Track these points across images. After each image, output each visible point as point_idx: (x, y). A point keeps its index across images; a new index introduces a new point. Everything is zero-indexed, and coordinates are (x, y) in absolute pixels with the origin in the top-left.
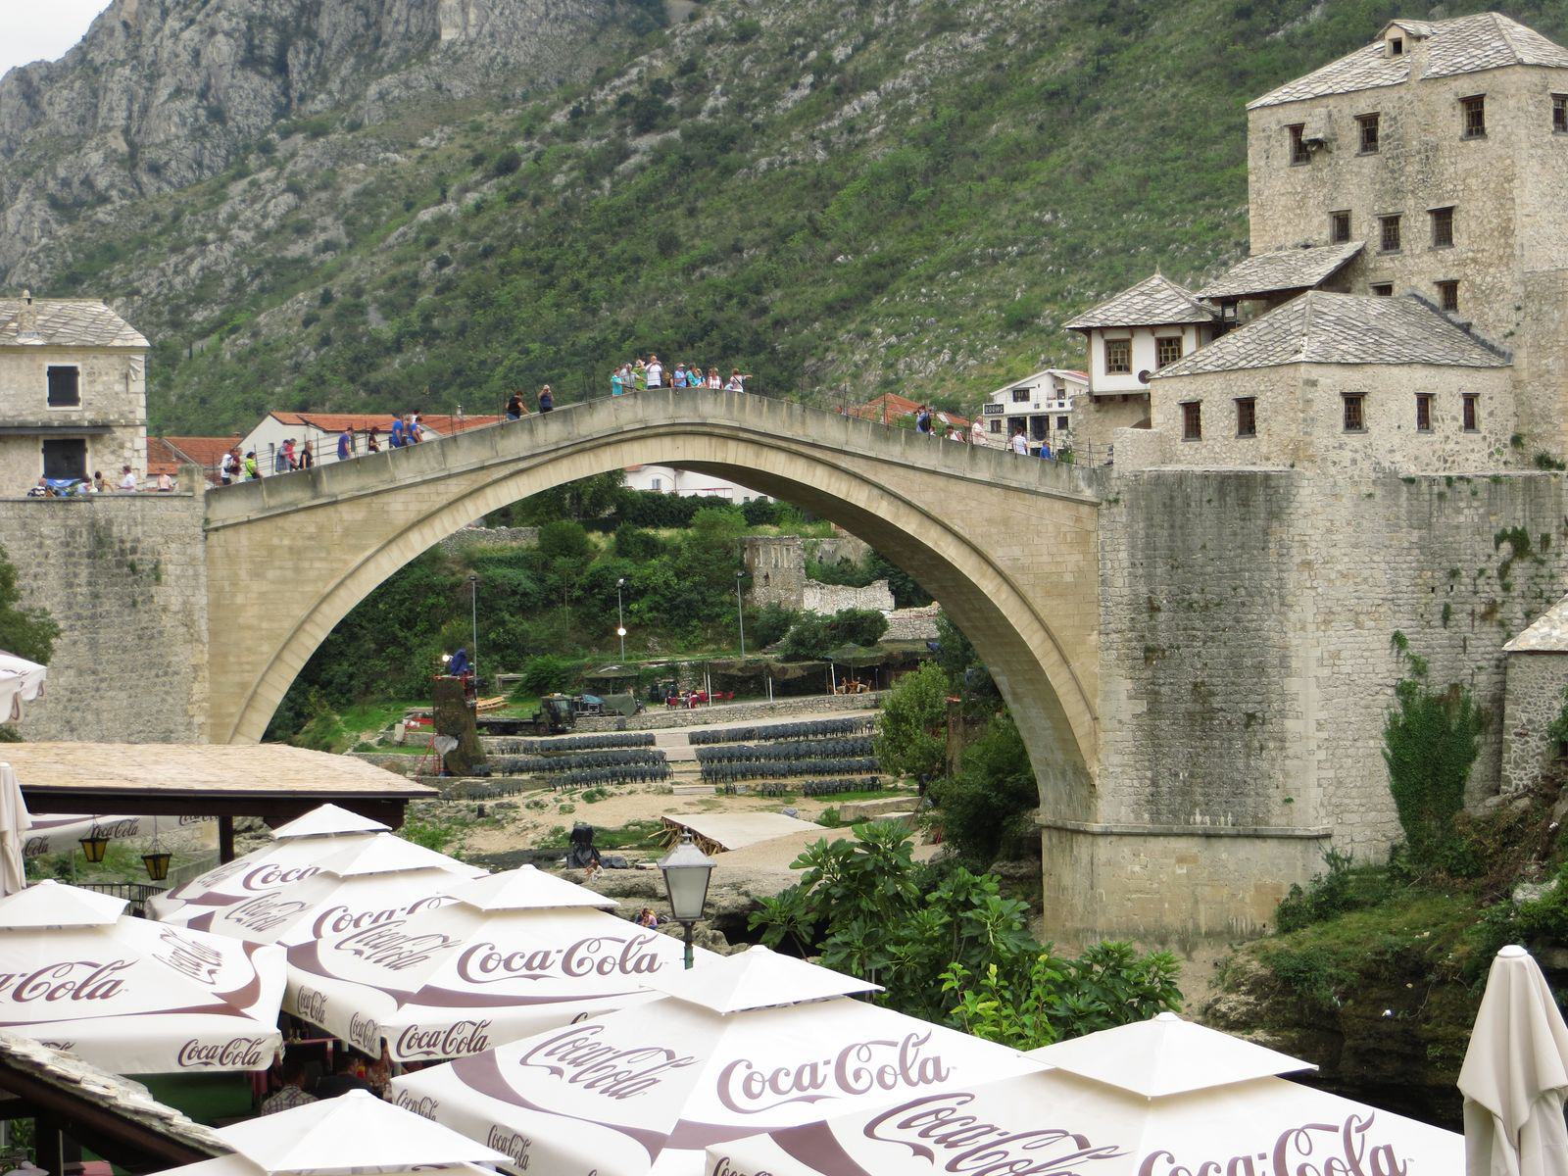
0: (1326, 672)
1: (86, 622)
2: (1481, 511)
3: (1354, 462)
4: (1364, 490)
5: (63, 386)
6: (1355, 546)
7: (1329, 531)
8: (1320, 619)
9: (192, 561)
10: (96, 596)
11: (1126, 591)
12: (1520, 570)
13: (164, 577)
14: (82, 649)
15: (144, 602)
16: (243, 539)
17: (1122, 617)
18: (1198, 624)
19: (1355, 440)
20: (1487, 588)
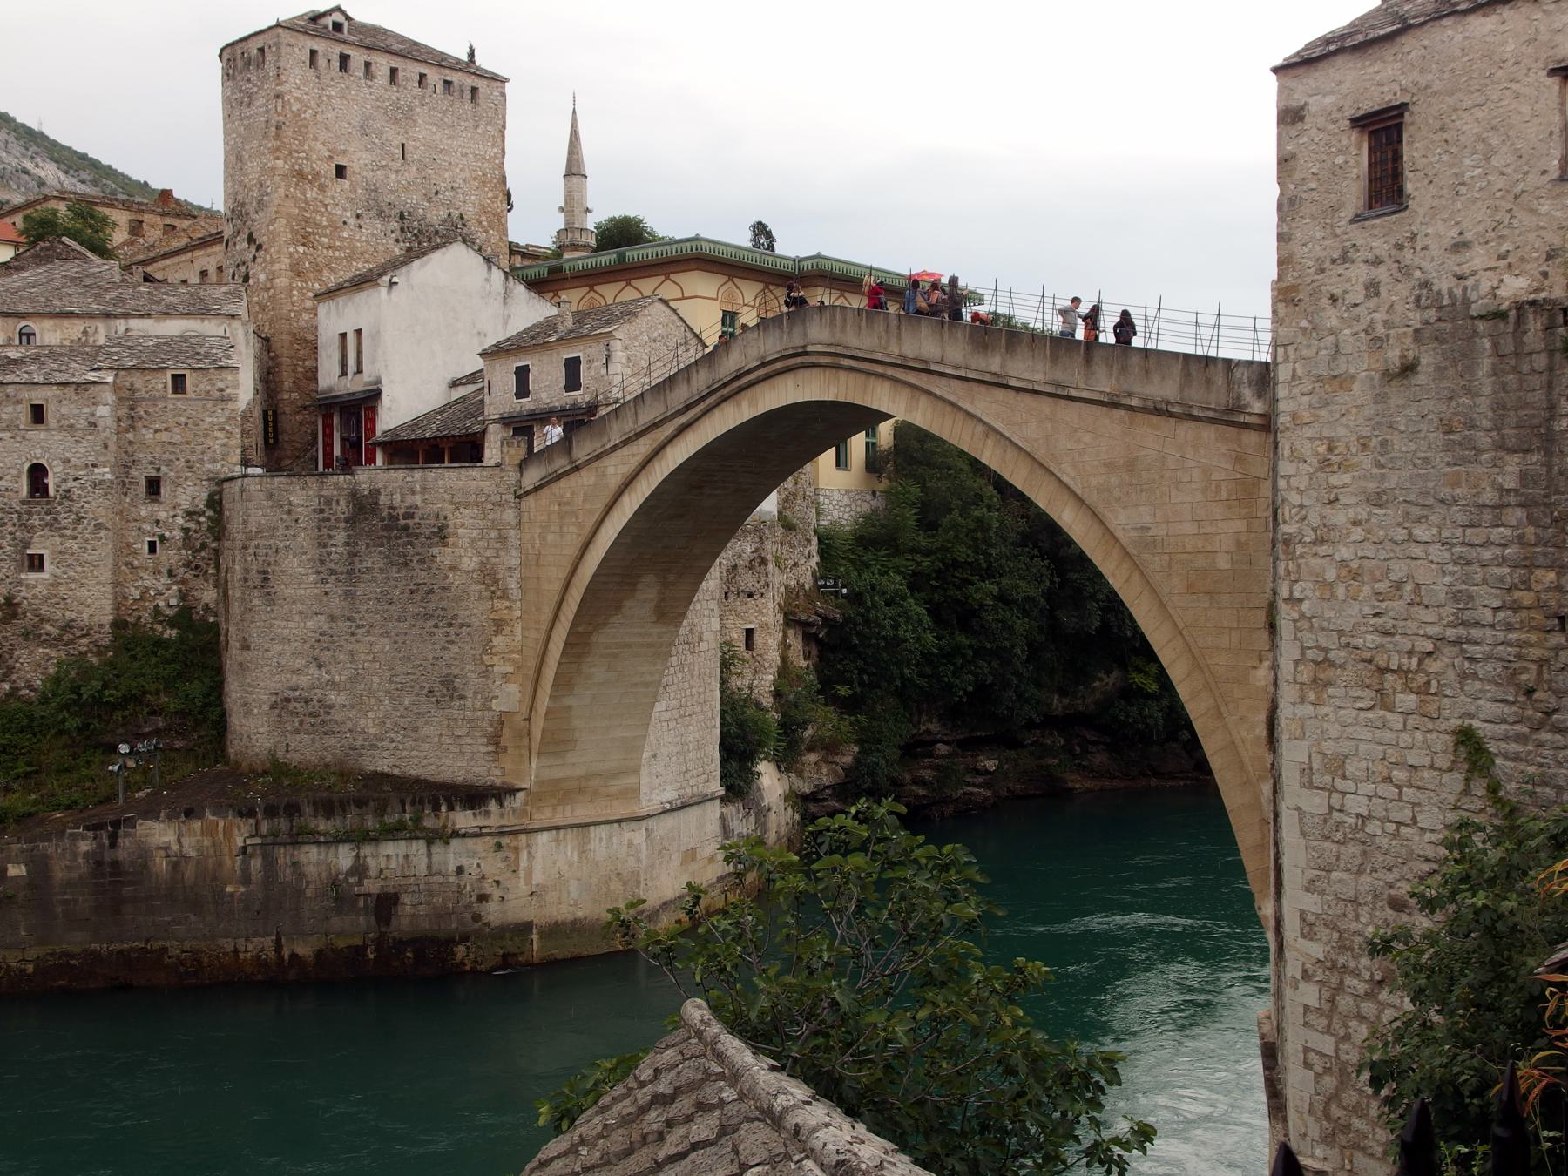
1: (341, 577)
3: (1373, 288)
4: (1393, 356)
7: (1324, 464)
8: (1306, 674)
10: (353, 554)
13: (450, 541)
19: (1378, 237)
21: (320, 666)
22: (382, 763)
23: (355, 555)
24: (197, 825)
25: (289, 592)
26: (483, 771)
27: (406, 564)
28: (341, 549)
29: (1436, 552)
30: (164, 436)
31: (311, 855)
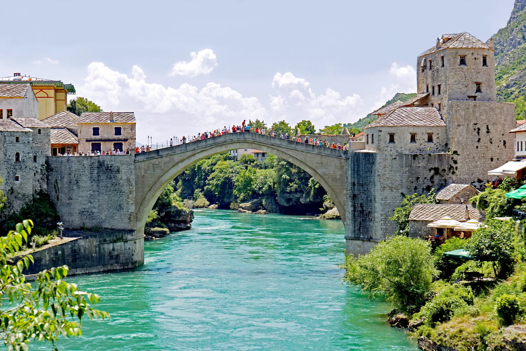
0: (383, 202)
2: (426, 163)
3: (391, 150)
4: (394, 157)
5: (118, 131)
6: (391, 171)
7: (384, 167)
9: (130, 169)
11: (350, 181)
12: (437, 179)
13: (120, 173)
14: (95, 187)
15: (114, 177)
16: (142, 165)
17: (350, 186)
18: (361, 189)
19: (392, 145)
20: (427, 182)
21: (91, 203)
22: (106, 226)
23: (99, 176)
24: (88, 240)
25: (83, 185)
26: (127, 226)
27: (111, 178)
28: (96, 175)
29: (399, 176)
30: (37, 145)
31: (106, 246)
